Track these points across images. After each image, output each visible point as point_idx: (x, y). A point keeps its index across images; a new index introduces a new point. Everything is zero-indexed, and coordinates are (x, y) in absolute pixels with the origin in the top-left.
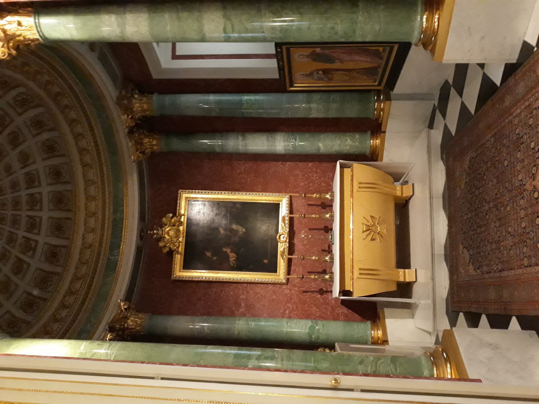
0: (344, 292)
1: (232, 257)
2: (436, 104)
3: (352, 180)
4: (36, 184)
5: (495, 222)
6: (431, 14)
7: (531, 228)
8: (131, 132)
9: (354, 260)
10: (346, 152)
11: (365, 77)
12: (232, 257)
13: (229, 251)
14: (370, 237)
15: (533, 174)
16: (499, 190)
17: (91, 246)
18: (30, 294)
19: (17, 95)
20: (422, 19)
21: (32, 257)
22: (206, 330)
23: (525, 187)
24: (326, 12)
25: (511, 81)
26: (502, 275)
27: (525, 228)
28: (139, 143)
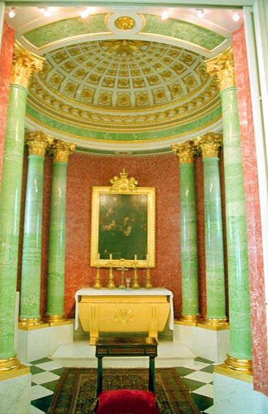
0: (80, 297)
4: (151, 83)
8: (191, 143)
17: (113, 121)
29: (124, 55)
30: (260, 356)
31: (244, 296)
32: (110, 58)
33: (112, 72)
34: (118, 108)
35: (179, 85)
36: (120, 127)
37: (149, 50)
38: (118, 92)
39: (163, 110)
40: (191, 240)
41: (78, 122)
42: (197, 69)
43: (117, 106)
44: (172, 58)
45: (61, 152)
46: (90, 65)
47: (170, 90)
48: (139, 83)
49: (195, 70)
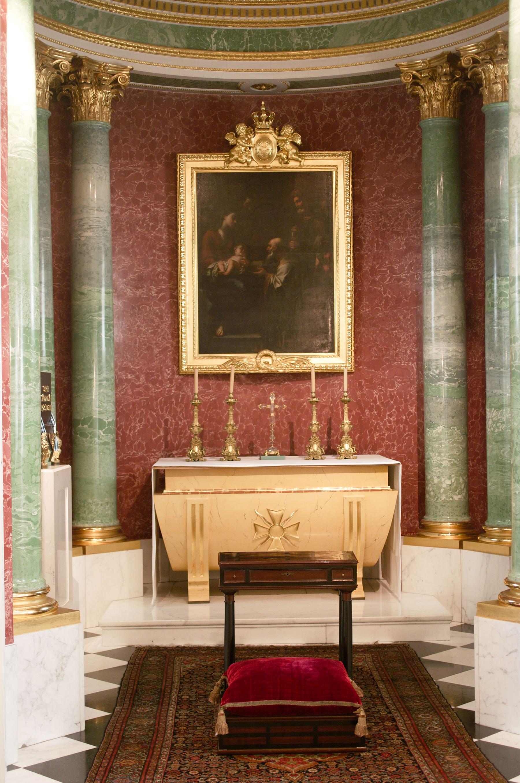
8: (453, 59)
10: (429, 477)
12: (226, 266)
13: (236, 259)
14: (260, 522)
22: (86, 234)
36: (255, 13)
40: (447, 327)
45: (91, 93)
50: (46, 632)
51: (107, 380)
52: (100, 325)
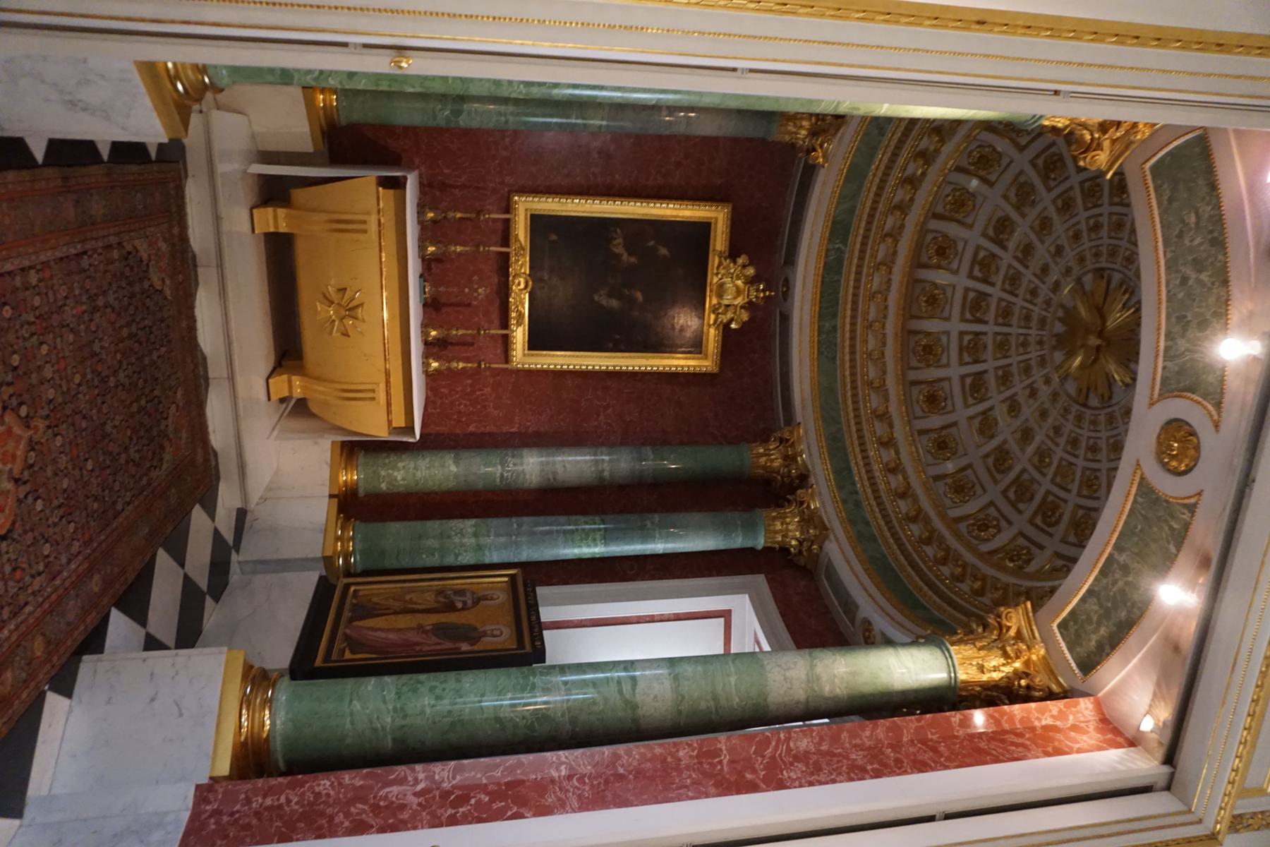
0: (396, 184)
1: (618, 247)
2: (234, 553)
3: (389, 405)
4: (968, 381)
5: (102, 348)
6: (256, 730)
7: (28, 344)
9: (377, 249)
11: (375, 600)
12: (618, 247)
13: (625, 257)
14: (348, 295)
15: (33, 449)
16: (99, 411)
17: (877, 267)
18: (984, 180)
19: (994, 536)
20: (273, 724)
21: (978, 248)
23: (47, 423)
24: (453, 724)
25: (92, 619)
26: (79, 246)
27: (41, 343)
28: (790, 459)
29: (1059, 328)
30: (289, 801)
31: (434, 723)
32: (1056, 287)
33: (1013, 280)
34: (913, 282)
35: (954, 454)
36: (856, 288)
37: (1064, 398)
38: (954, 287)
39: (893, 408)
40: (555, 473)
41: (886, 174)
42: (992, 511)
43: (917, 281)
44: (1030, 449)
46: (1044, 225)
47: (944, 428)
48: (972, 348)
49: (992, 504)
50: (142, 88)
51: (507, 122)
52: (567, 117)
